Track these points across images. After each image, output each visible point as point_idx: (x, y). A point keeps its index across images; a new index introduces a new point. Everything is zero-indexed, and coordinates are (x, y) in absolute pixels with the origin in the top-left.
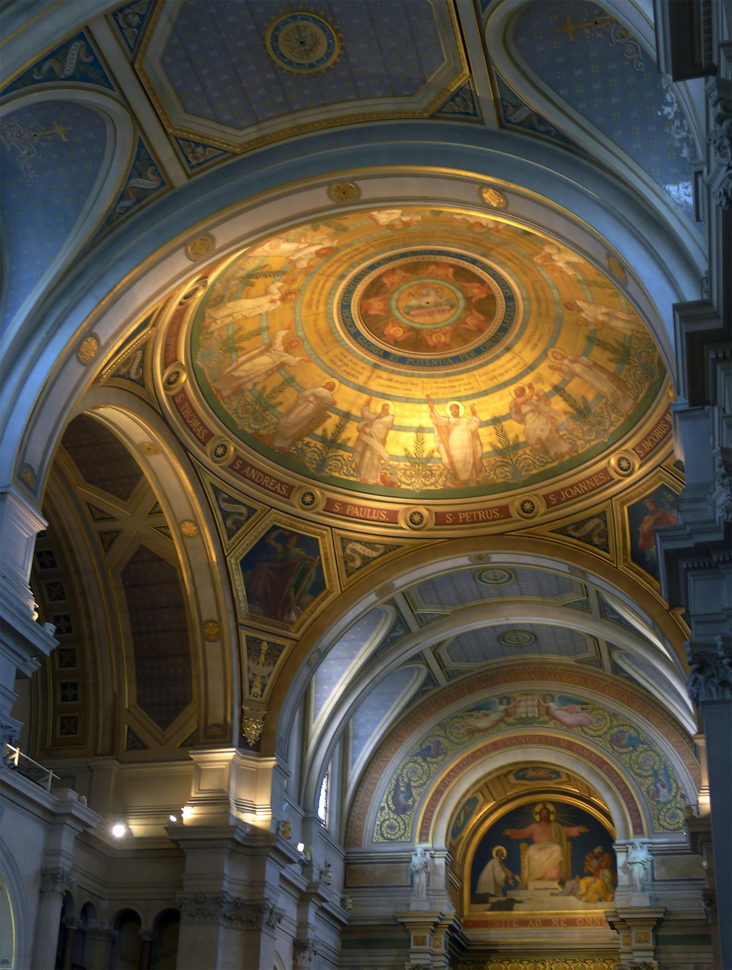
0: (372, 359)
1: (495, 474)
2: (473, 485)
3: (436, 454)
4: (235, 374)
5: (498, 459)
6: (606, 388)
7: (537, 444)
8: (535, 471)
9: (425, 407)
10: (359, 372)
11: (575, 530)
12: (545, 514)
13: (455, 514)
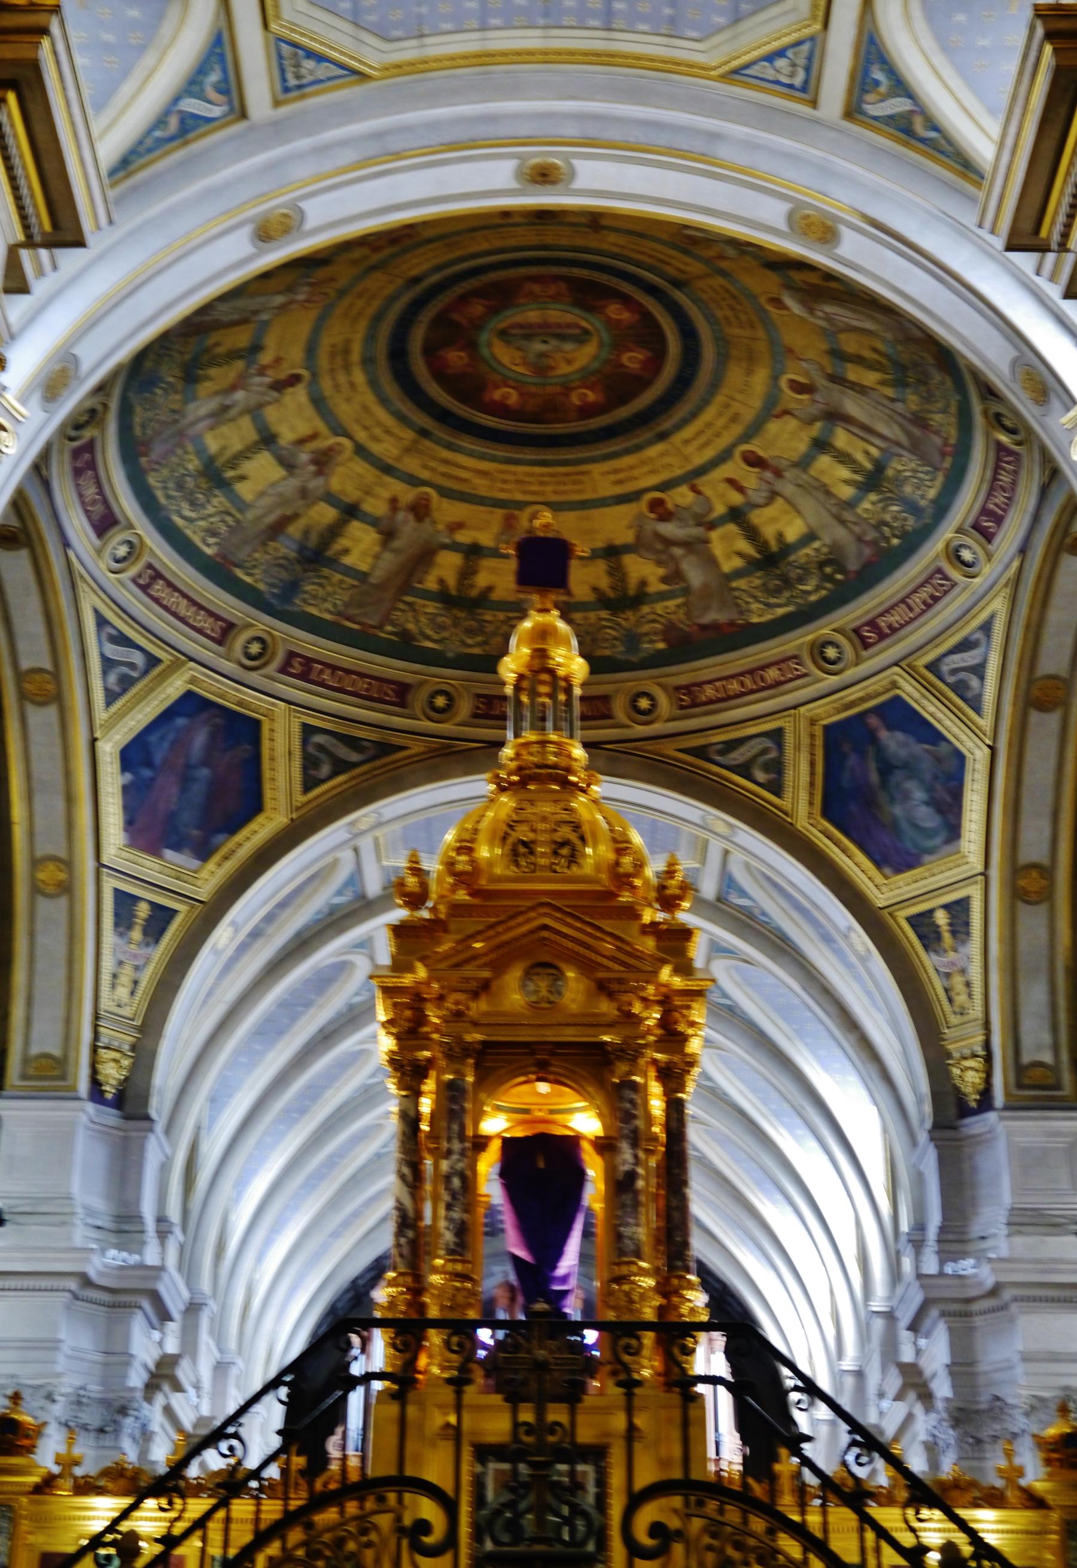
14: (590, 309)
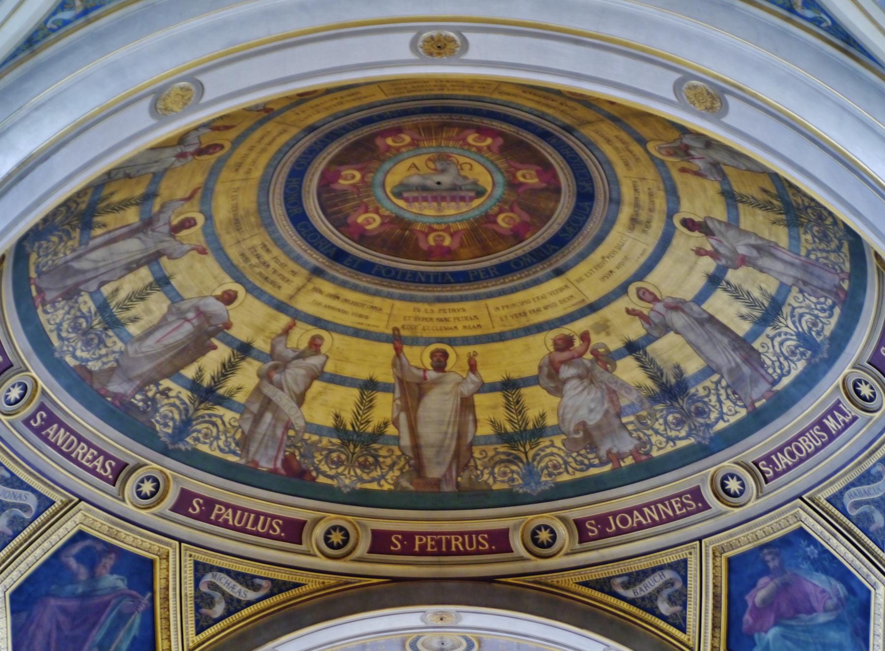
0: (316, 259)
1: (492, 474)
2: (447, 488)
3: (391, 430)
4: (76, 265)
5: (502, 449)
6: (726, 358)
7: (576, 432)
8: (565, 477)
9: (388, 349)
10: (283, 278)
11: (626, 586)
12: (574, 552)
13: (408, 537)
14: (397, 221)
